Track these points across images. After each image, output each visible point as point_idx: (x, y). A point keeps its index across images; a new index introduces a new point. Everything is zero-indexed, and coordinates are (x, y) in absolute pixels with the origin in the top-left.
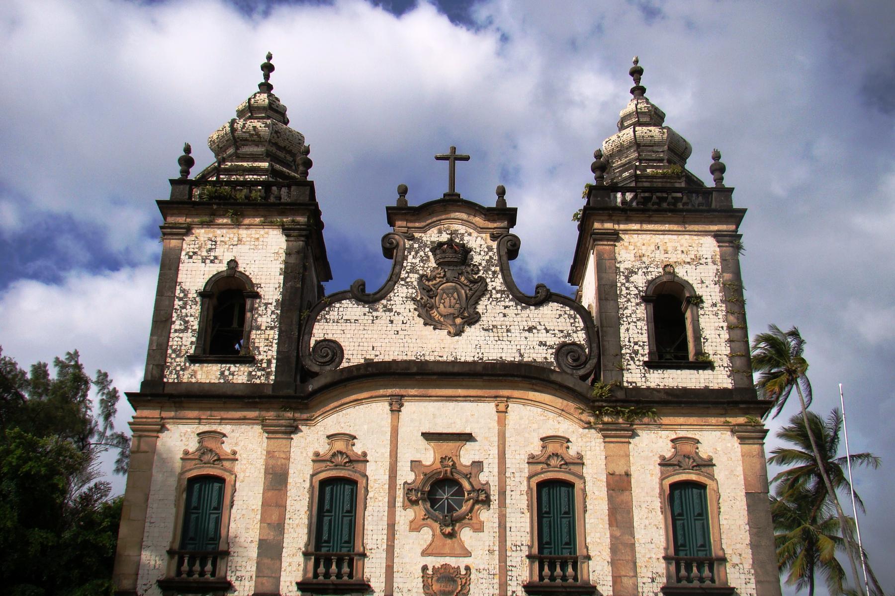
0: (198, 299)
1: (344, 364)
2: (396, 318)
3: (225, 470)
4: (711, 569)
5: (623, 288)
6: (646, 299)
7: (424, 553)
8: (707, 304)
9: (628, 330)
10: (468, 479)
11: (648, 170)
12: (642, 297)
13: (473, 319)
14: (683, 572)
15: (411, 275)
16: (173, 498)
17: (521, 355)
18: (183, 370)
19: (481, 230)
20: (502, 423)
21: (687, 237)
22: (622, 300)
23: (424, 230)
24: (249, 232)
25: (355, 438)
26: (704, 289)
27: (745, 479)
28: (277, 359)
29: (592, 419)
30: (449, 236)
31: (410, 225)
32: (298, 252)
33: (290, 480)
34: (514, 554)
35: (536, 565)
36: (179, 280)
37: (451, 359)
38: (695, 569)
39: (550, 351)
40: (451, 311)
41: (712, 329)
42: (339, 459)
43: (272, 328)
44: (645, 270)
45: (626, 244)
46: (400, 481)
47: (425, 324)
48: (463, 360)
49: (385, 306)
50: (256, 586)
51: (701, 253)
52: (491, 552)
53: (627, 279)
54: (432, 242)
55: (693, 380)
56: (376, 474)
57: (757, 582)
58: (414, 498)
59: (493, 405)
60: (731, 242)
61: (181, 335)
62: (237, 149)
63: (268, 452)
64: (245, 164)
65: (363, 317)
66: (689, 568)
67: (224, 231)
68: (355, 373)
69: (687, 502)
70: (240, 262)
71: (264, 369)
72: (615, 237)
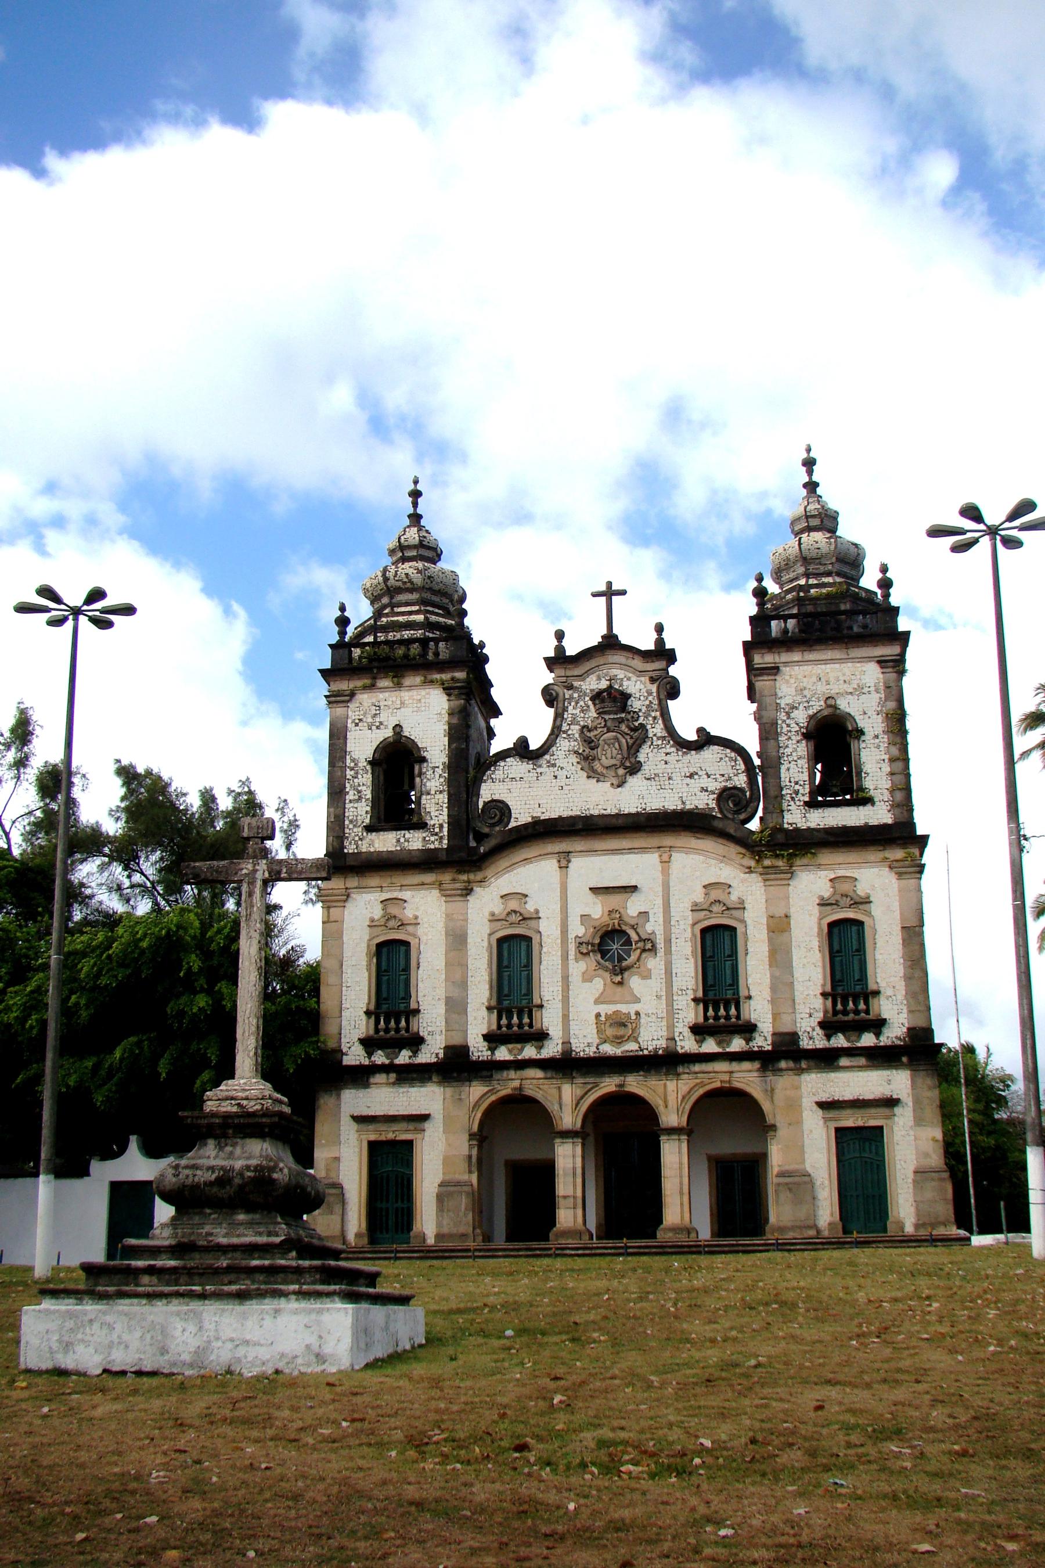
0: (369, 767)
2: (559, 773)
3: (409, 934)
4: (867, 1003)
5: (784, 725)
6: (807, 736)
7: (597, 1002)
8: (868, 737)
9: (788, 769)
10: (635, 930)
11: (812, 591)
12: (803, 734)
14: (839, 1007)
15: (572, 727)
16: (365, 963)
17: (683, 803)
18: (361, 839)
20: (666, 873)
21: (850, 665)
22: (782, 738)
23: (582, 677)
24: (411, 693)
26: (867, 720)
27: (901, 914)
29: (752, 863)
30: (608, 683)
31: (569, 673)
32: (460, 712)
34: (680, 998)
35: (701, 1006)
37: (615, 811)
38: (851, 1003)
40: (613, 762)
42: (514, 918)
43: (441, 792)
45: (787, 677)
46: (571, 936)
47: (588, 777)
49: (548, 762)
53: (788, 714)
54: (592, 690)
55: (853, 818)
56: (549, 930)
57: (910, 1012)
58: (585, 951)
59: (656, 855)
60: (893, 667)
62: (392, 598)
64: (401, 619)
65: (527, 774)
66: (845, 1004)
67: (387, 694)
68: (524, 833)
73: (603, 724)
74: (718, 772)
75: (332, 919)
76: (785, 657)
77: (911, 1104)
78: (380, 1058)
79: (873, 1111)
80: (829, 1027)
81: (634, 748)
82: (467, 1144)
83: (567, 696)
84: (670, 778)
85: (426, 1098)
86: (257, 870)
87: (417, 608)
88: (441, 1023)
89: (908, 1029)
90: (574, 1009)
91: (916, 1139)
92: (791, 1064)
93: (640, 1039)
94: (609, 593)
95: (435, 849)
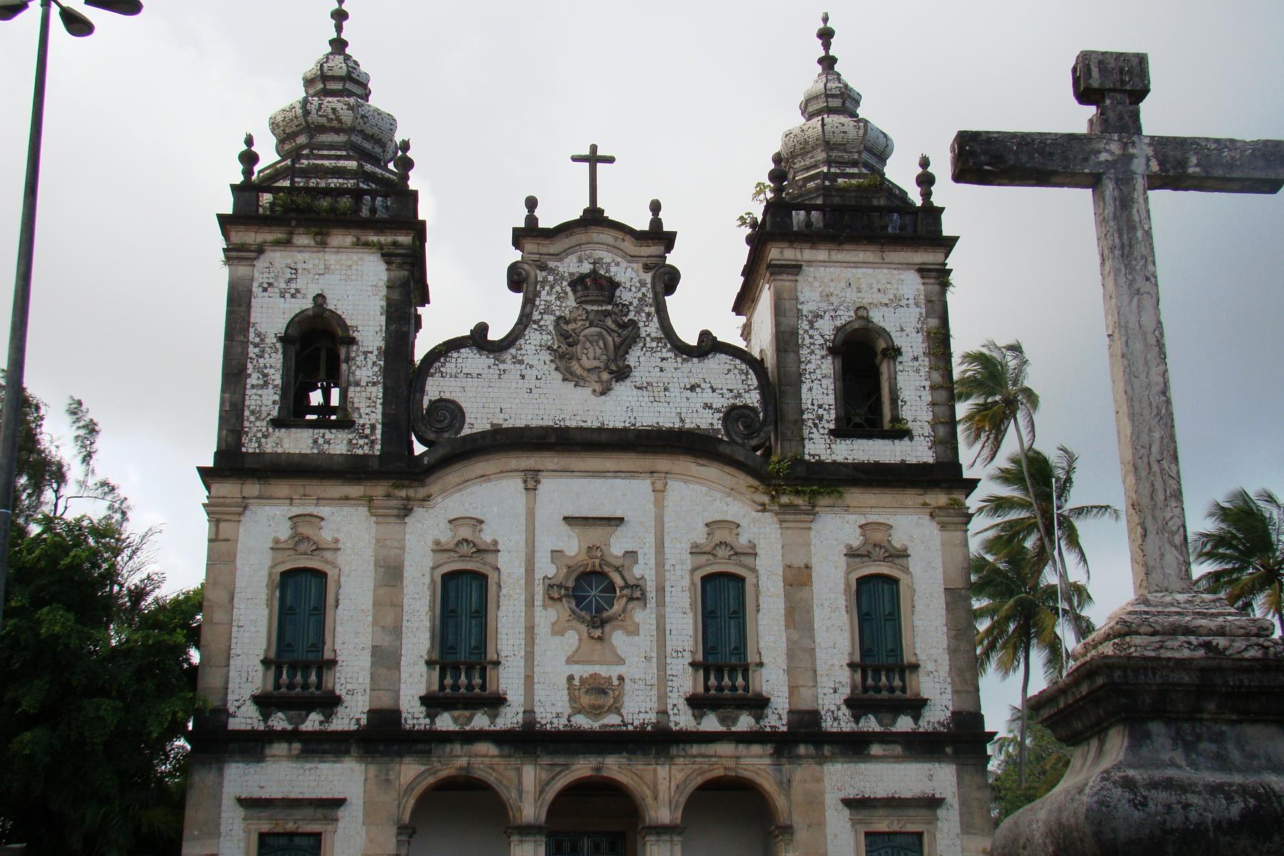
0: (279, 345)
2: (528, 372)
3: (327, 562)
4: (902, 679)
5: (806, 337)
6: (833, 351)
7: (570, 661)
8: (906, 357)
9: (811, 389)
10: (620, 573)
11: (840, 180)
12: (829, 348)
13: (622, 374)
14: (870, 682)
15: (545, 317)
16: (264, 597)
17: (682, 421)
18: (265, 436)
20: (659, 504)
21: (885, 271)
23: (559, 256)
24: (339, 256)
25: (481, 522)
26: (904, 338)
28: (383, 424)
29: (766, 499)
31: (543, 250)
33: (406, 575)
35: (701, 672)
36: (252, 320)
37: (596, 424)
38: (883, 678)
39: (718, 415)
40: (596, 363)
41: (912, 390)
42: (465, 549)
43: (374, 384)
44: (833, 314)
46: (539, 575)
47: (564, 380)
48: (611, 426)
50: (371, 701)
51: (901, 292)
53: (811, 323)
54: (571, 274)
56: (510, 566)
57: (955, 692)
58: (556, 596)
61: (260, 392)
62: (311, 137)
63: (378, 541)
64: (326, 163)
65: (486, 371)
67: (306, 255)
69: (877, 601)
70: (328, 296)
71: (366, 437)
72: (795, 268)
73: (584, 317)
74: (725, 387)
75: (221, 536)
76: (808, 254)
77: (956, 806)
78: (279, 722)
79: (911, 812)
80: (857, 705)
81: (623, 348)
82: (394, 840)
83: (540, 279)
84: (666, 389)
85: (343, 778)
86: (1132, 156)
87: (344, 153)
88: (364, 678)
89: (953, 713)
90: (539, 667)
91: (963, 850)
92: (811, 750)
93: (624, 711)
94: (593, 159)
95: (365, 455)
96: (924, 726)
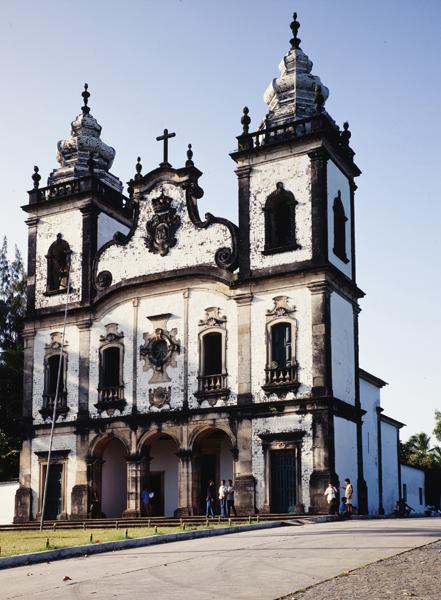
1: (113, 284)
7: (150, 383)
19: (177, 184)
46: (138, 346)
52: (180, 377)
69: (279, 337)
76: (255, 160)
80: (269, 389)
90: (139, 387)
94: (166, 137)
96: (299, 396)
